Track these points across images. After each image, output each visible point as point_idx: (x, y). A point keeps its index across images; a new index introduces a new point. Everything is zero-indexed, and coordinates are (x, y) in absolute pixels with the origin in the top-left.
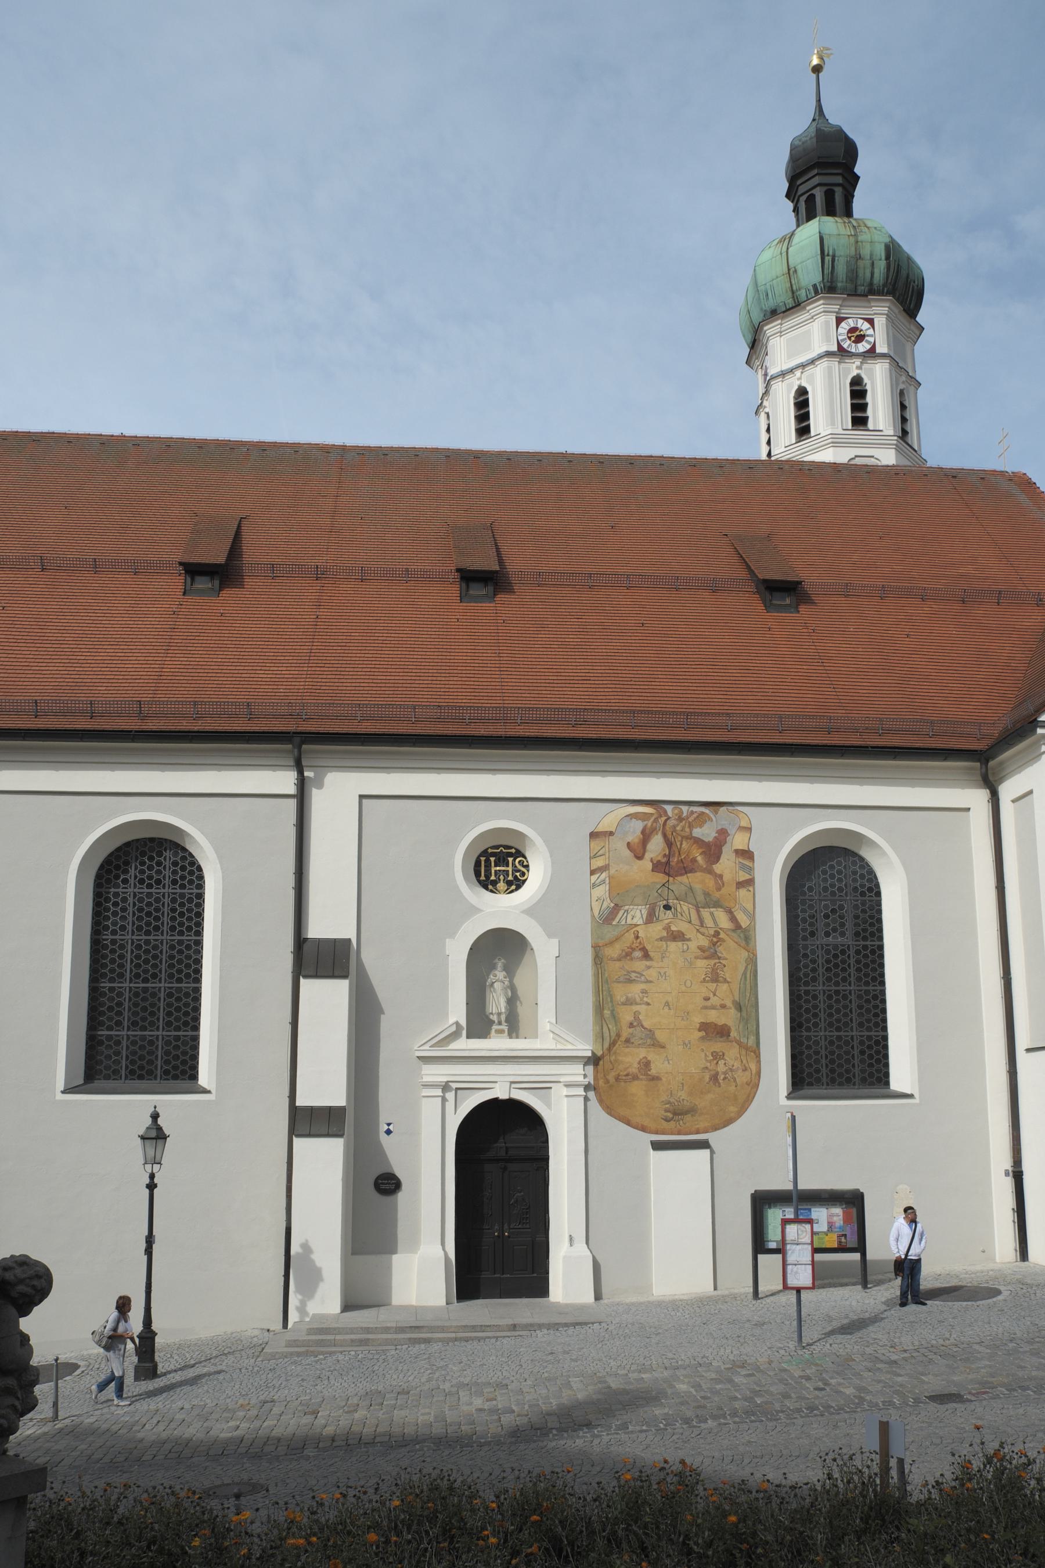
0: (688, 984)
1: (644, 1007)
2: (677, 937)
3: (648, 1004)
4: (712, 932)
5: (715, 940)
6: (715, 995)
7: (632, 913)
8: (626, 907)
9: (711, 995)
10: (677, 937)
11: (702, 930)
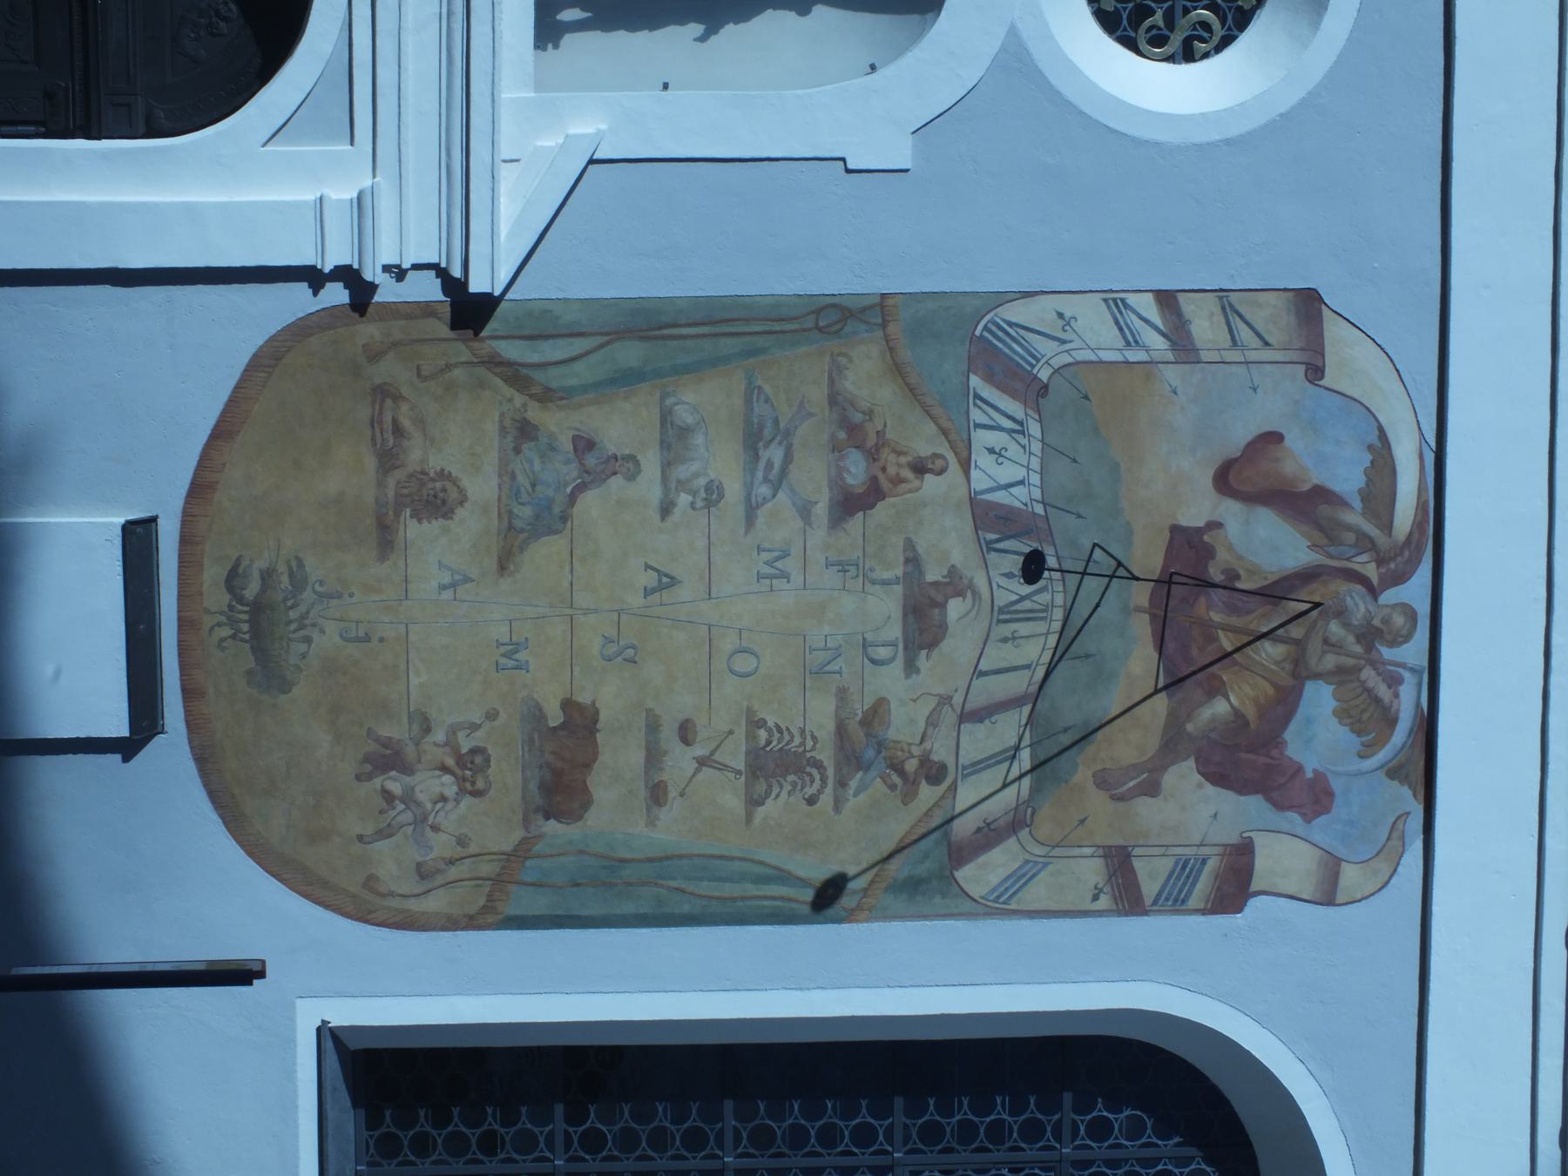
0: (744, 663)
1: (655, 494)
2: (923, 623)
3: (666, 510)
4: (941, 752)
5: (911, 766)
6: (702, 762)
7: (1013, 450)
8: (1034, 429)
9: (699, 751)
10: (923, 623)
11: (949, 717)
